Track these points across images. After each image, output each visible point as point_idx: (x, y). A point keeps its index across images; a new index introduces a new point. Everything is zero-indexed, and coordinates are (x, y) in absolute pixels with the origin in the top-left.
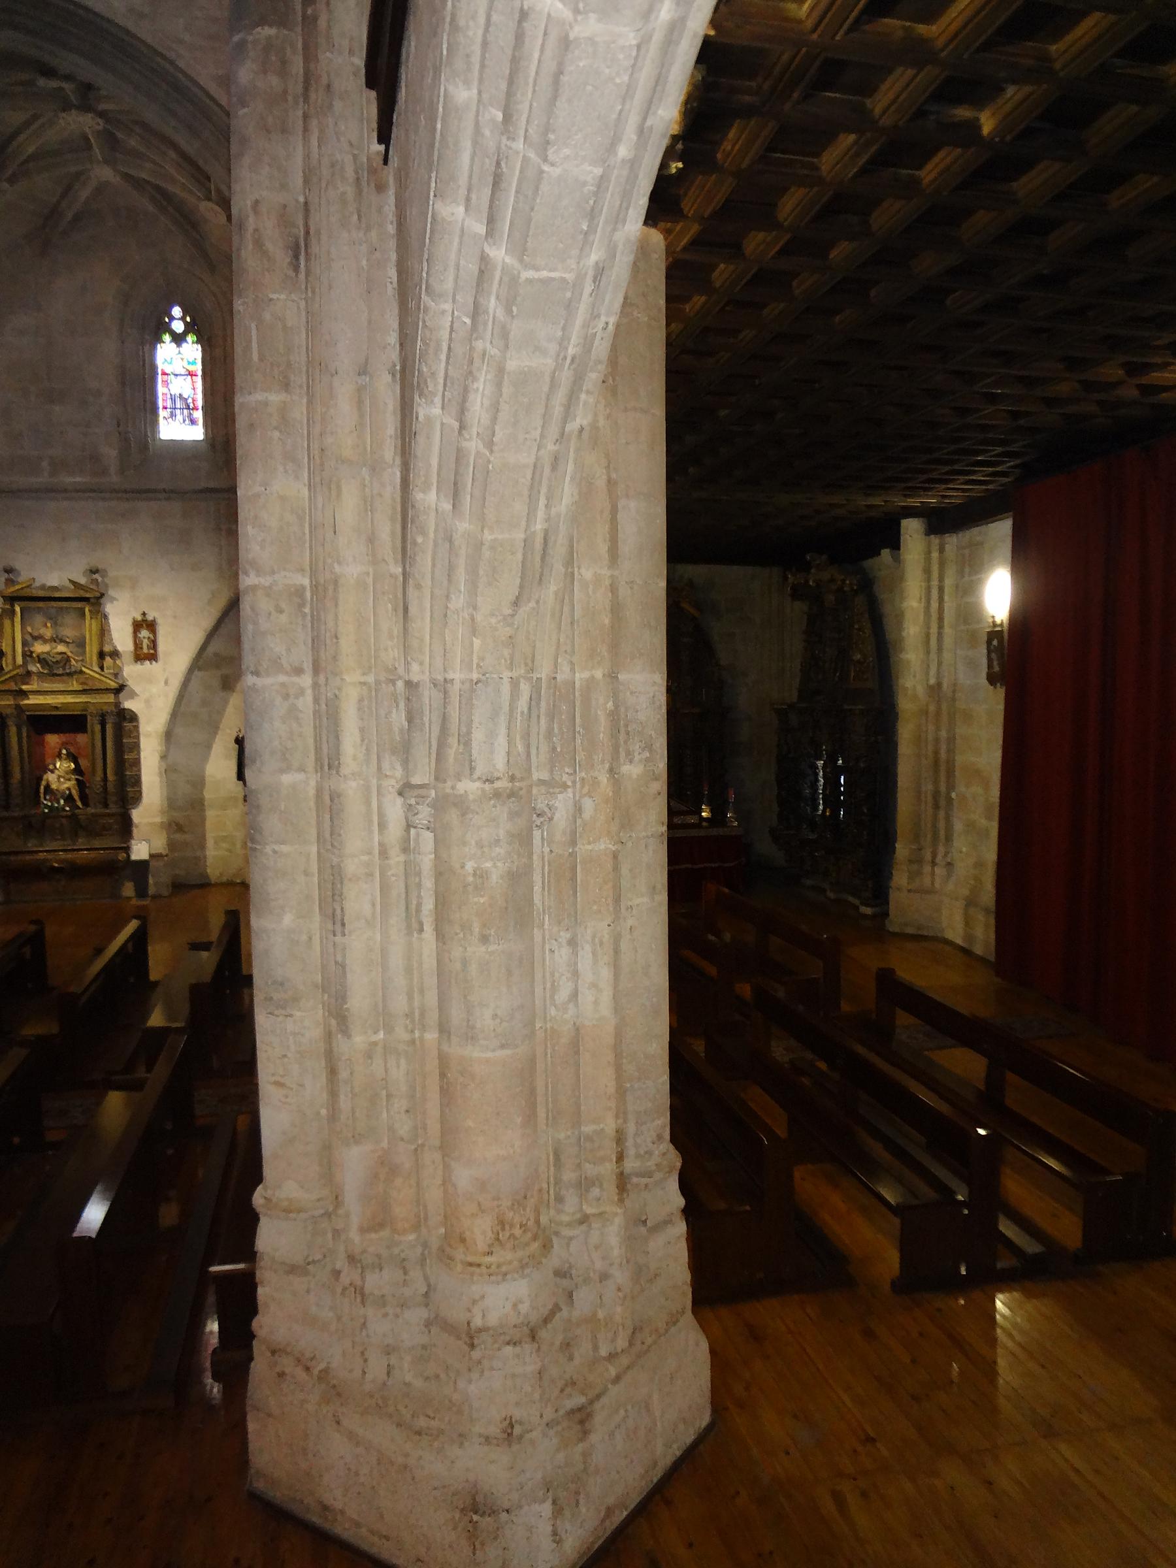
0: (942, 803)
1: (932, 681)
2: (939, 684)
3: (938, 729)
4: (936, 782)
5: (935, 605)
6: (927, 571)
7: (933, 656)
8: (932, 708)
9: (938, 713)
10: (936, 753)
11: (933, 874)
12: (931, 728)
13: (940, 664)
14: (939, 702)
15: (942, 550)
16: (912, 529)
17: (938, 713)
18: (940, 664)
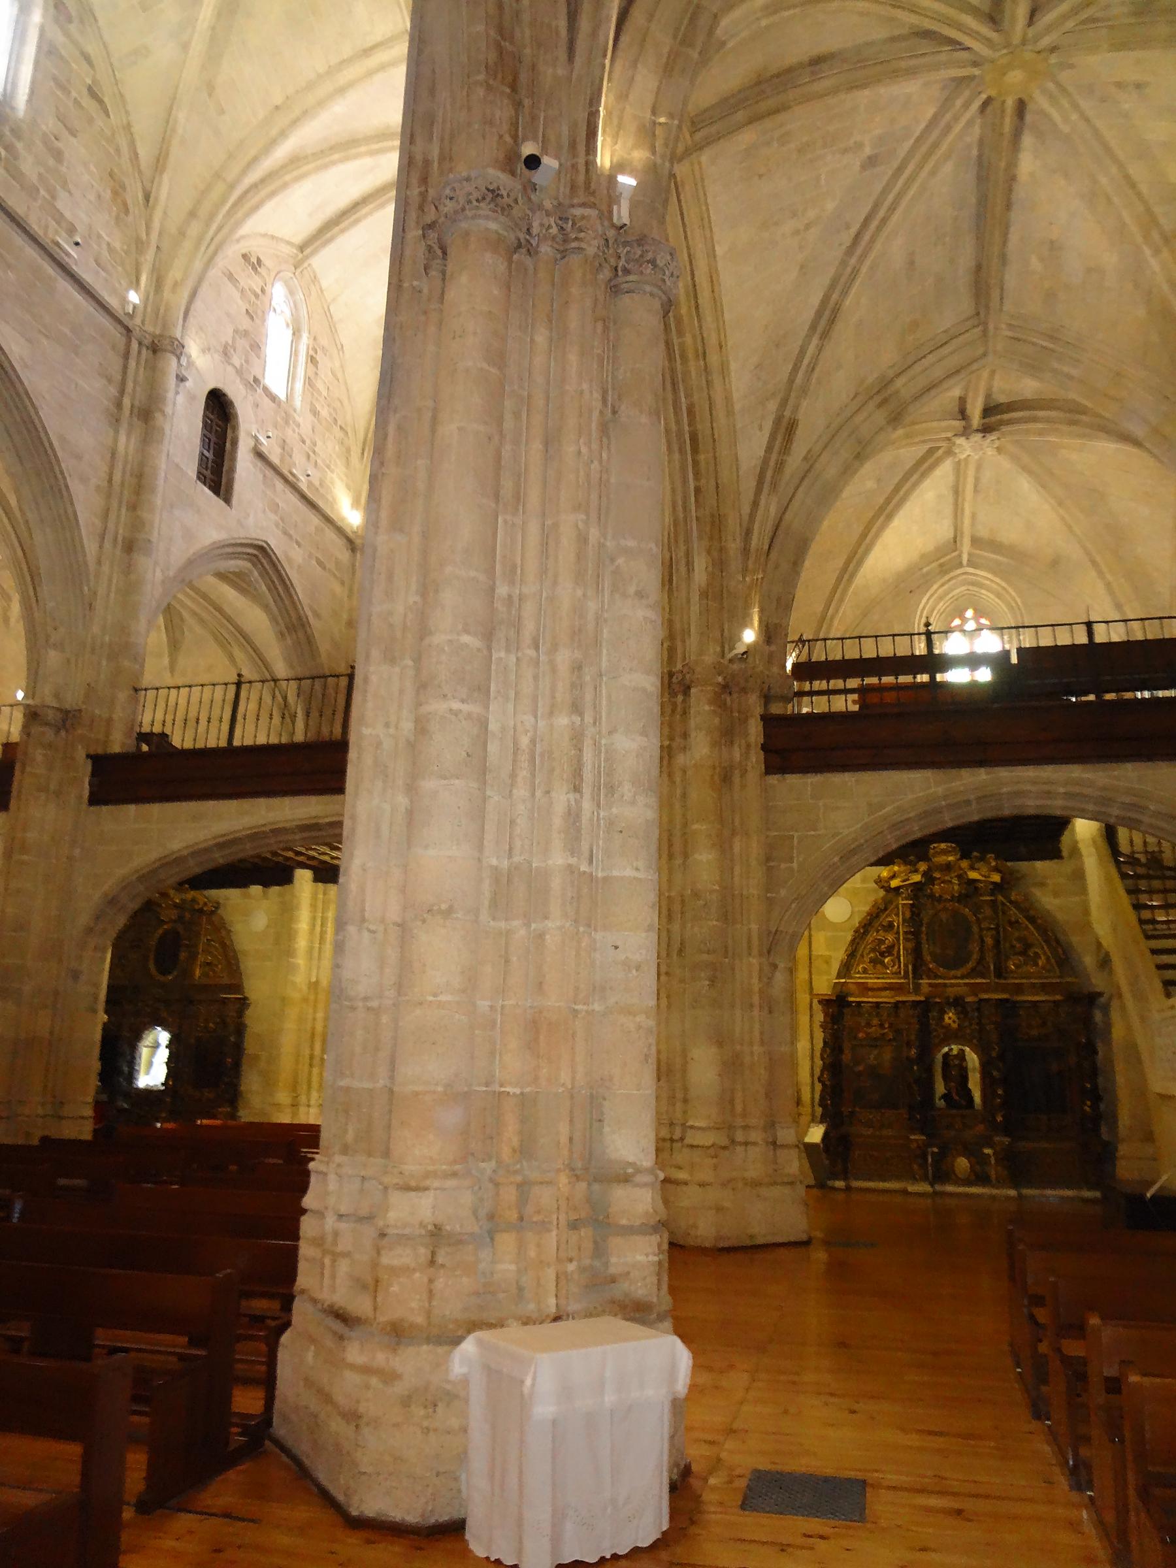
0: (316, 1061)
1: (314, 979)
2: (317, 983)
3: (315, 1012)
4: (312, 1048)
5: (318, 929)
6: (313, 906)
7: (315, 962)
8: (312, 997)
9: (316, 1001)
10: (313, 1028)
11: (308, 1113)
12: (311, 1011)
13: (319, 968)
14: (317, 994)
15: (325, 894)
16: (303, 876)
17: (316, 1001)
18: (319, 968)
